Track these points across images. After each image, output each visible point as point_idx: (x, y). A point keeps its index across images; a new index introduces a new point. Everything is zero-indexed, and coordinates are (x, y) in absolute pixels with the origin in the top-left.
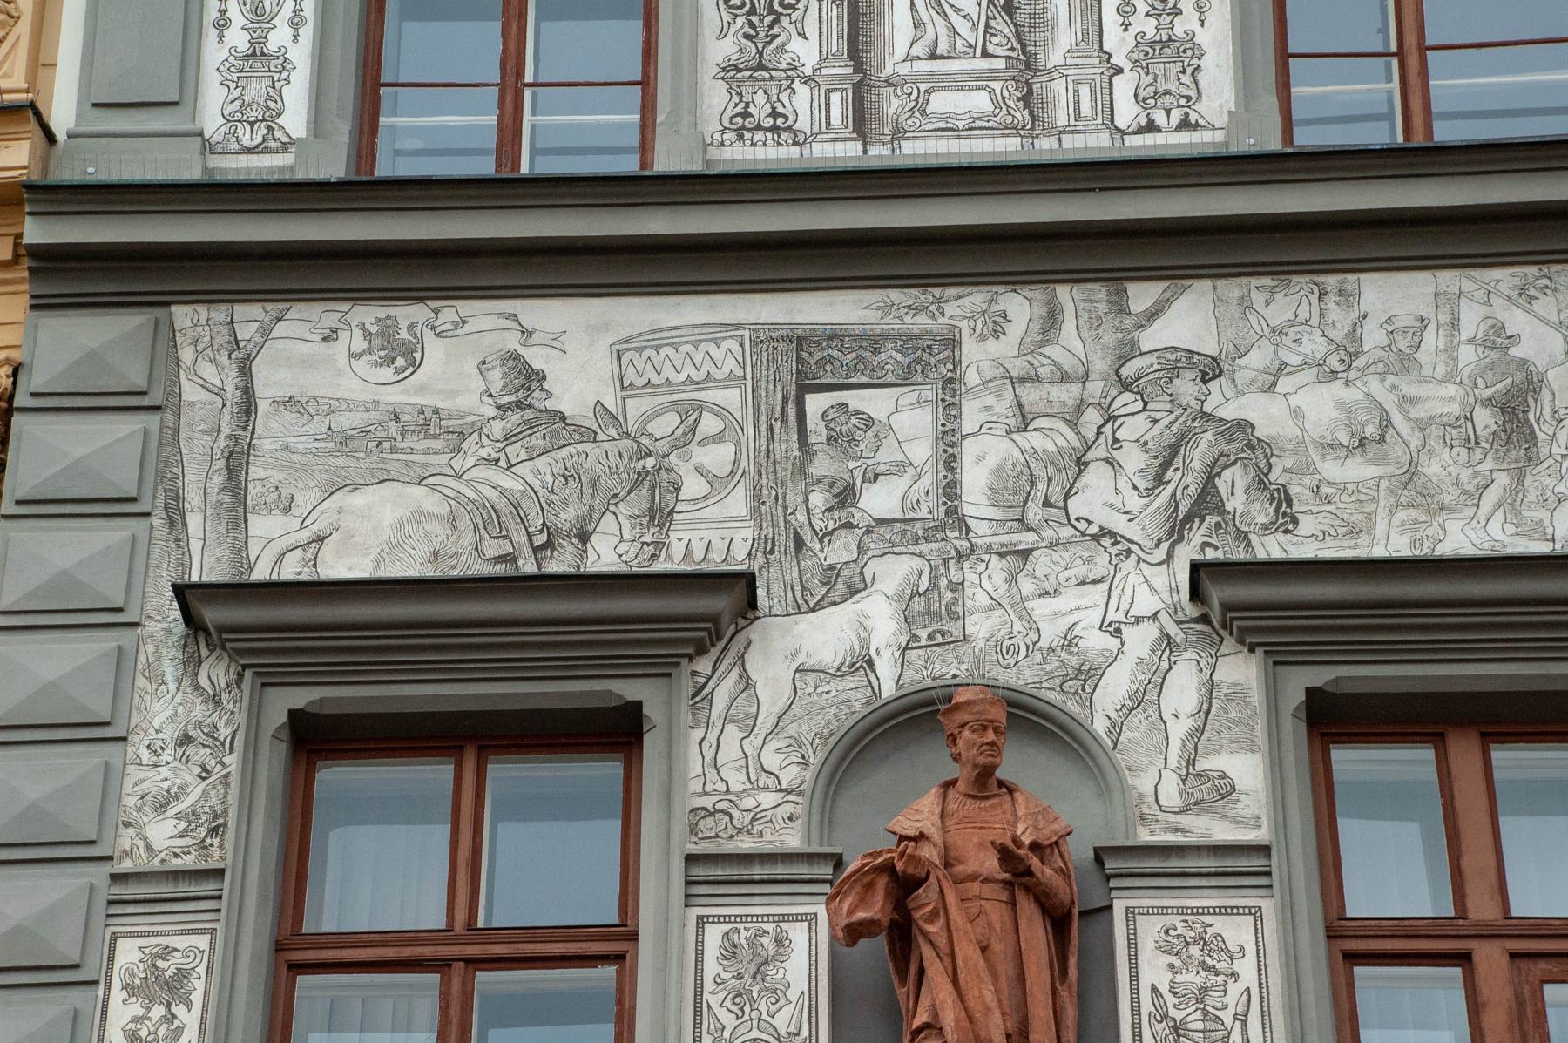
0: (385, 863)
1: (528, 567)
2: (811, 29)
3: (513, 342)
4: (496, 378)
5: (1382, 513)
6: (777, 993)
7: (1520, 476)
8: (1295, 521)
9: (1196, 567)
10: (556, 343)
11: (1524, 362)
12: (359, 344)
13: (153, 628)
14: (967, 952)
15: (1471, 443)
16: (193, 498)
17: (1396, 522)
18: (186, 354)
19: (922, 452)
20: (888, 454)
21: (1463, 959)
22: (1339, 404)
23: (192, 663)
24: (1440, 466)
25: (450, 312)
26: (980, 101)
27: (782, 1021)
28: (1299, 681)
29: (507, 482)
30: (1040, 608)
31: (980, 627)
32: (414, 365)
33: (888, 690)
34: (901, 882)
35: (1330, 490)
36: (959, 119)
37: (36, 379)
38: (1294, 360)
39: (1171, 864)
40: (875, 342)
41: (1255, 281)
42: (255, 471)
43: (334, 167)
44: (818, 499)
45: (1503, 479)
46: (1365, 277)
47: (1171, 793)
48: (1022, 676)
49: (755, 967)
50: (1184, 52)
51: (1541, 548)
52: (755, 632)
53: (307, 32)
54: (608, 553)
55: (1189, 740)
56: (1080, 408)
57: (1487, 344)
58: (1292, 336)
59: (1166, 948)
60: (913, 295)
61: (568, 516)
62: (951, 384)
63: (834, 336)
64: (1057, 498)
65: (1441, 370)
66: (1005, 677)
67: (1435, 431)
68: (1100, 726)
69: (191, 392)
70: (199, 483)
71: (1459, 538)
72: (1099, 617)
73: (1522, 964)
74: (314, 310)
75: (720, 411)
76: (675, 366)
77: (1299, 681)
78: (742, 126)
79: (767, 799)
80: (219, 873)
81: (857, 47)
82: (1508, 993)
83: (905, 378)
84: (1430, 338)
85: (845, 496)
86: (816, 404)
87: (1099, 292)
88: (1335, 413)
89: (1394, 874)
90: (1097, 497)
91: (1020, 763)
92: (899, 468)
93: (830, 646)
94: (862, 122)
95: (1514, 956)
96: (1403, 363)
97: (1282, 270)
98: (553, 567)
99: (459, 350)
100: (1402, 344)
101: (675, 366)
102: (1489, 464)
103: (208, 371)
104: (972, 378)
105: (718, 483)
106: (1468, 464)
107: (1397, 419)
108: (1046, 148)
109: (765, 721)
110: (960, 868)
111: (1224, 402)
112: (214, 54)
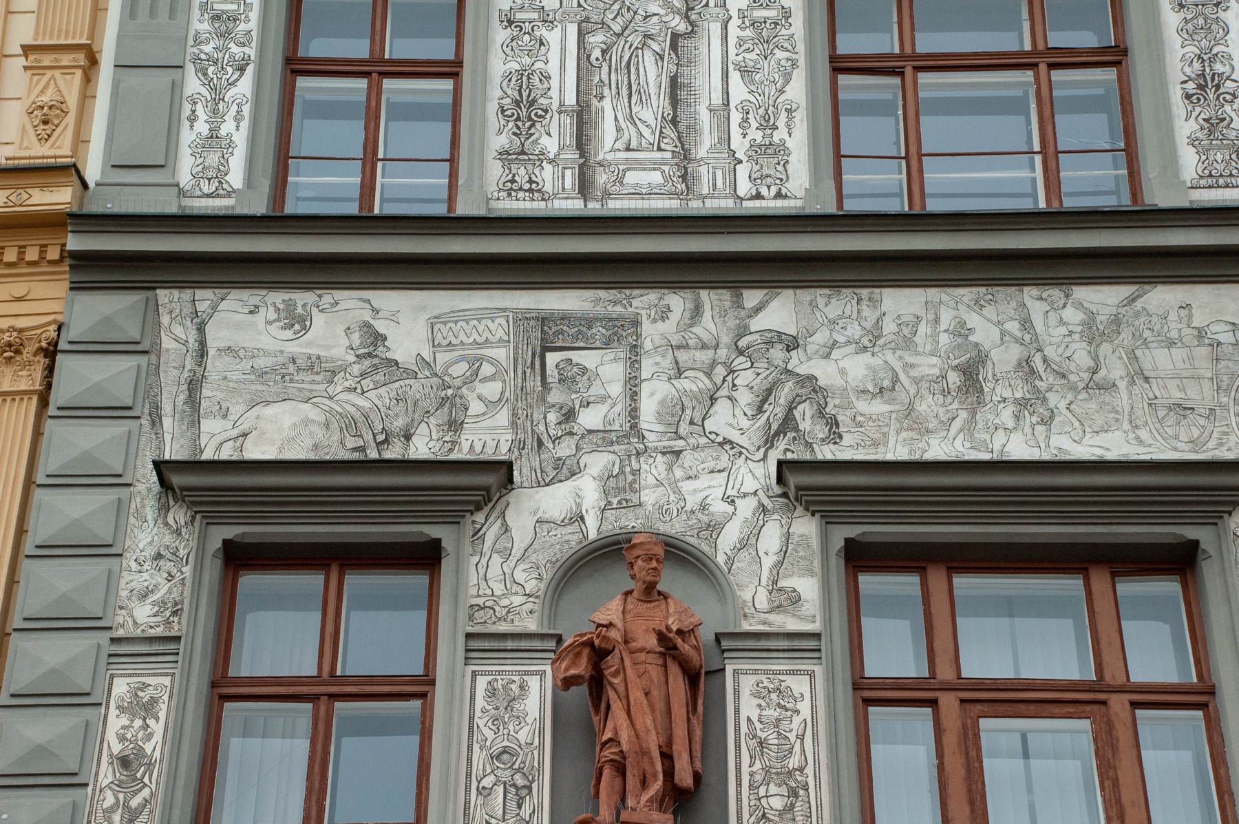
0: (280, 635)
1: (373, 454)
2: (554, 130)
3: (367, 316)
4: (356, 339)
5: (892, 433)
6: (520, 719)
7: (973, 413)
8: (841, 437)
9: (781, 464)
10: (393, 318)
11: (977, 345)
12: (272, 315)
13: (141, 487)
14: (636, 695)
15: (945, 392)
16: (167, 408)
17: (900, 439)
18: (165, 320)
19: (616, 389)
20: (596, 390)
21: (933, 703)
22: (869, 367)
23: (164, 509)
24: (927, 406)
25: (328, 297)
26: (656, 177)
27: (523, 736)
28: (841, 534)
29: (361, 402)
30: (686, 486)
31: (649, 497)
32: (306, 329)
33: (592, 535)
34: (598, 652)
35: (861, 419)
36: (643, 187)
37: (72, 333)
38: (842, 339)
39: (761, 644)
40: (589, 322)
41: (819, 291)
42: (206, 392)
43: (259, 207)
44: (552, 417)
45: (963, 415)
46: (884, 290)
47: (762, 600)
48: (674, 527)
49: (506, 703)
50: (778, 152)
51: (985, 456)
52: (512, 497)
53: (245, 125)
54: (422, 447)
55: (774, 568)
56: (713, 364)
57: (956, 333)
58: (841, 325)
59: (757, 694)
60: (613, 294)
61: (398, 424)
62: (635, 349)
63: (565, 317)
64: (698, 420)
65: (928, 348)
66: (664, 528)
67: (924, 385)
68: (721, 559)
69: (167, 343)
70: (171, 398)
71: (937, 451)
72: (723, 496)
73: (967, 706)
74: (245, 294)
75: (493, 361)
76: (466, 333)
77: (841, 534)
78: (511, 187)
79: (517, 600)
80: (177, 639)
81: (582, 142)
82: (959, 724)
83: (607, 344)
84: (923, 329)
85: (569, 415)
86: (552, 358)
87: (726, 295)
88: (866, 372)
89: (894, 652)
90: (722, 420)
91: (671, 580)
92: (603, 399)
93: (557, 507)
94: (584, 187)
95: (962, 701)
96: (906, 343)
97: (836, 285)
98: (389, 455)
99: (335, 321)
100: (906, 331)
101: (466, 333)
102: (955, 405)
103: (178, 330)
104: (648, 345)
105: (491, 405)
106: (943, 405)
107: (902, 377)
108: (695, 207)
109: (517, 552)
110: (633, 645)
111: (800, 364)
112: (187, 136)
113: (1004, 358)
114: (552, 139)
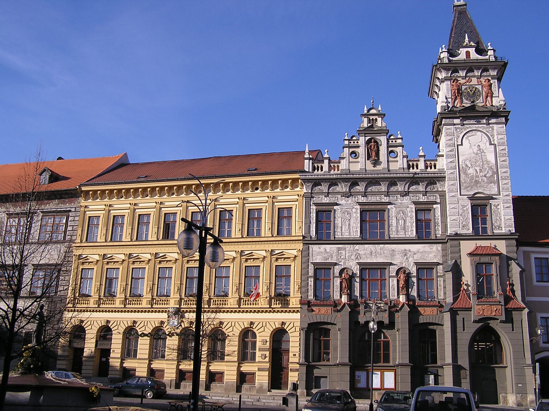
36: (346, 235)
113: (374, 252)
114: (339, 230)
